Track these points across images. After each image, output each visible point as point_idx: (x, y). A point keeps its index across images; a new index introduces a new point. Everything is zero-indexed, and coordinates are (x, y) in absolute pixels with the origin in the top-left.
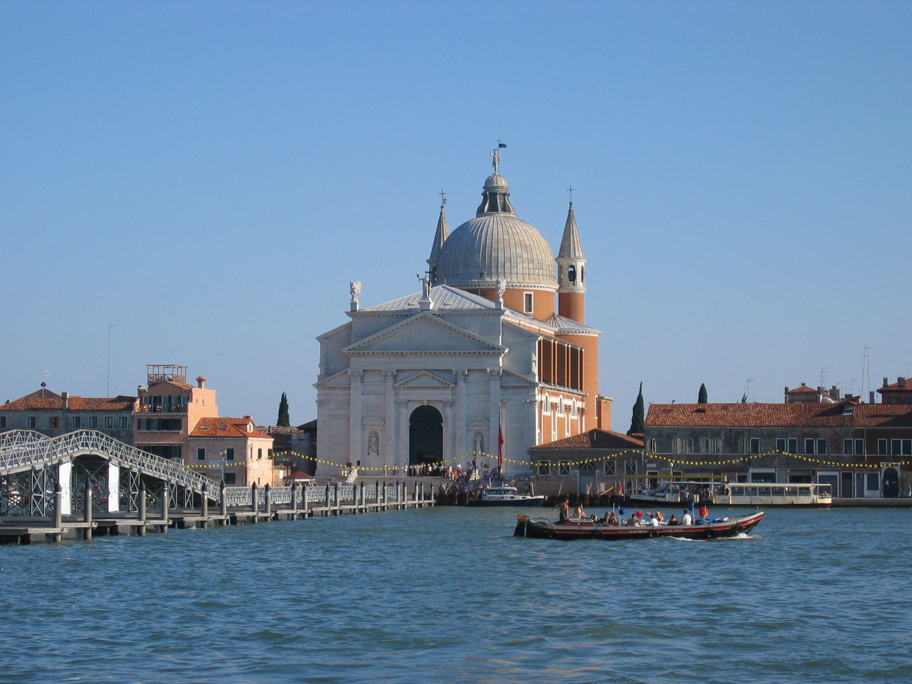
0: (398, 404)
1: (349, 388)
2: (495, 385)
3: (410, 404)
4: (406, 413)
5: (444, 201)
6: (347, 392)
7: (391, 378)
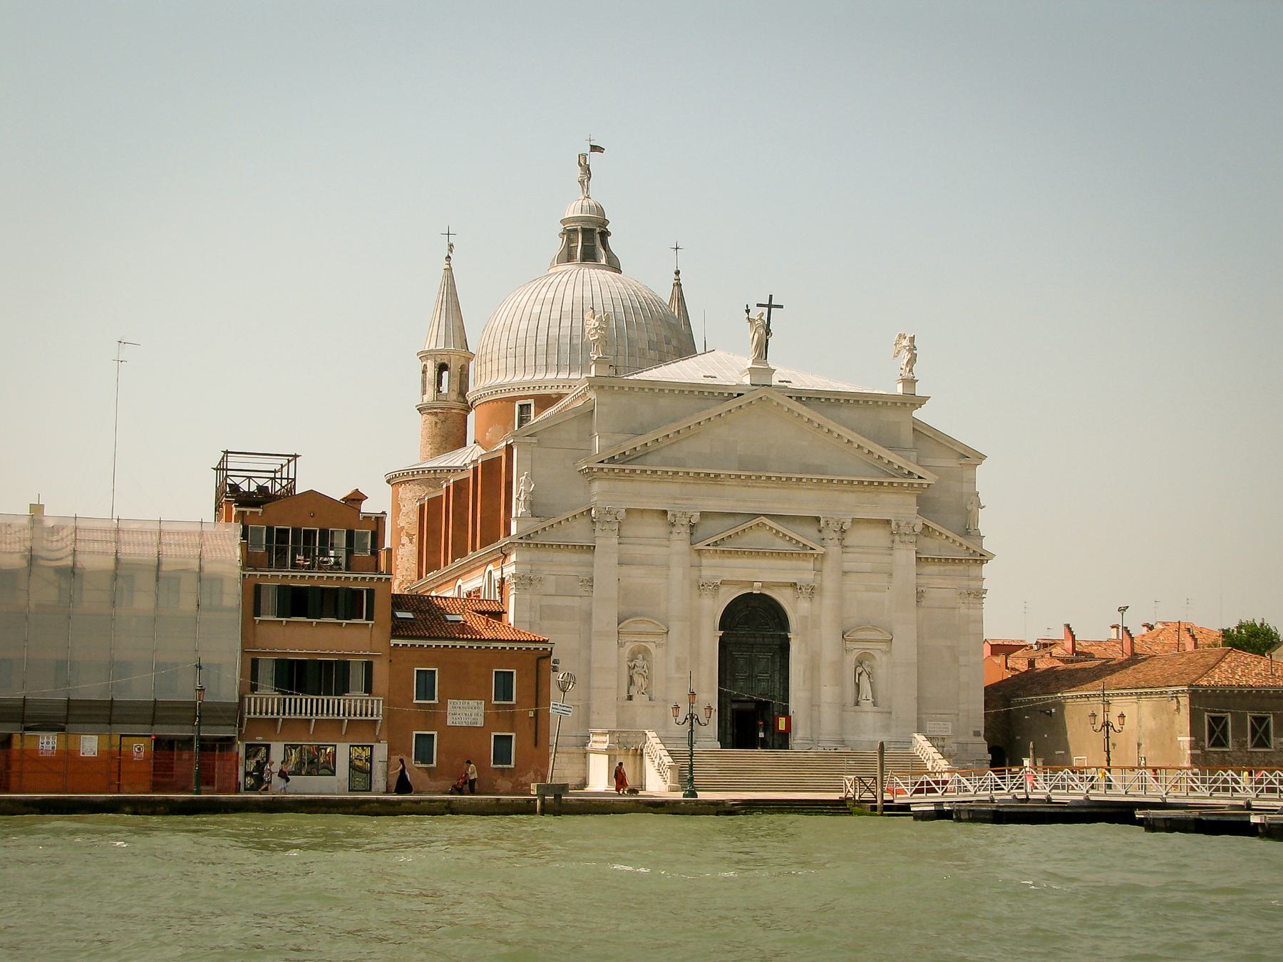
1: (591, 549)
2: (905, 555)
3: (723, 589)
4: (715, 606)
5: (451, 245)
6: (585, 557)
7: (684, 531)
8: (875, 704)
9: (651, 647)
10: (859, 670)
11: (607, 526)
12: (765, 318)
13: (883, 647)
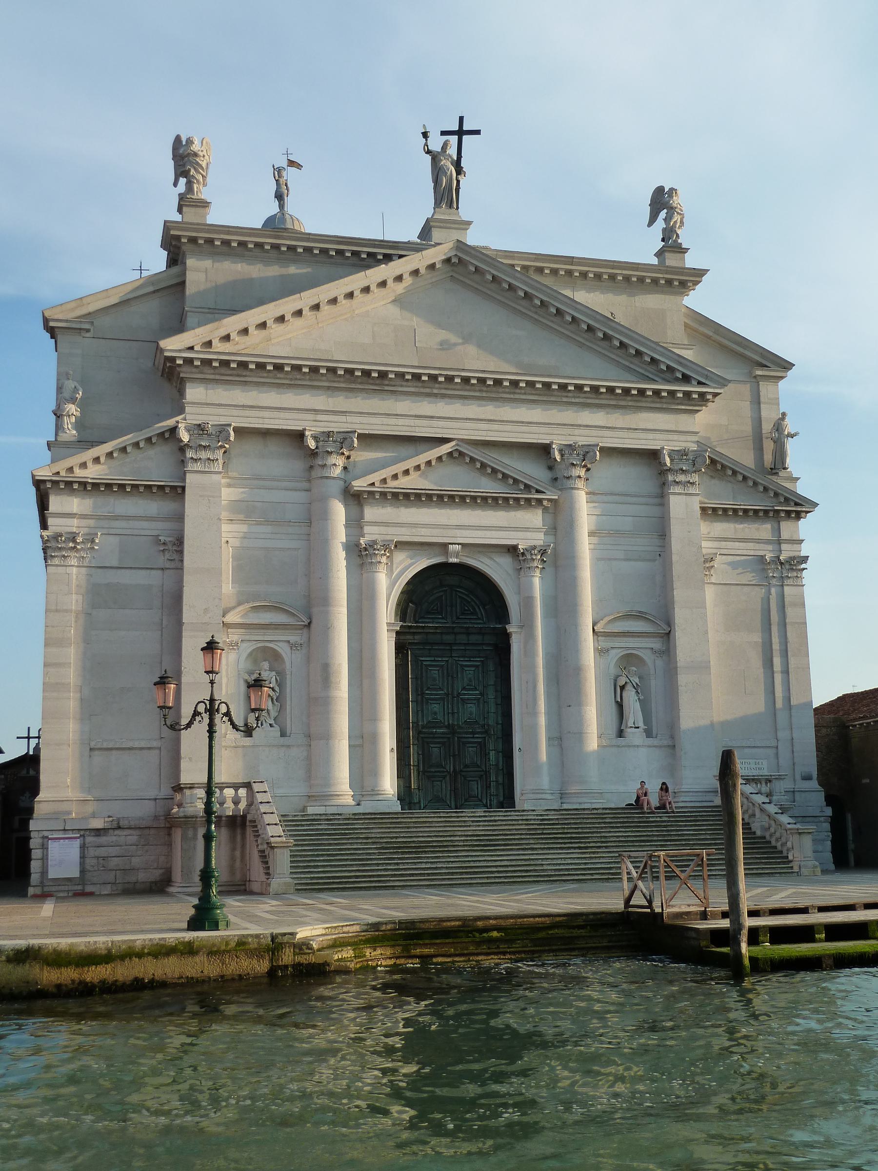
0: (361, 555)
4: (388, 584)
8: (649, 733)
9: (283, 650)
10: (622, 681)
11: (203, 455)
12: (453, 151)
13: (656, 644)
